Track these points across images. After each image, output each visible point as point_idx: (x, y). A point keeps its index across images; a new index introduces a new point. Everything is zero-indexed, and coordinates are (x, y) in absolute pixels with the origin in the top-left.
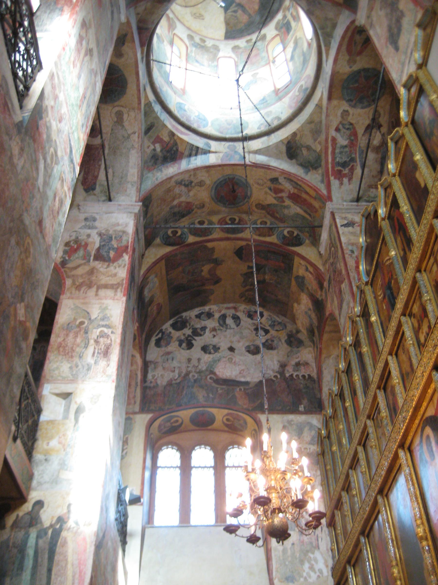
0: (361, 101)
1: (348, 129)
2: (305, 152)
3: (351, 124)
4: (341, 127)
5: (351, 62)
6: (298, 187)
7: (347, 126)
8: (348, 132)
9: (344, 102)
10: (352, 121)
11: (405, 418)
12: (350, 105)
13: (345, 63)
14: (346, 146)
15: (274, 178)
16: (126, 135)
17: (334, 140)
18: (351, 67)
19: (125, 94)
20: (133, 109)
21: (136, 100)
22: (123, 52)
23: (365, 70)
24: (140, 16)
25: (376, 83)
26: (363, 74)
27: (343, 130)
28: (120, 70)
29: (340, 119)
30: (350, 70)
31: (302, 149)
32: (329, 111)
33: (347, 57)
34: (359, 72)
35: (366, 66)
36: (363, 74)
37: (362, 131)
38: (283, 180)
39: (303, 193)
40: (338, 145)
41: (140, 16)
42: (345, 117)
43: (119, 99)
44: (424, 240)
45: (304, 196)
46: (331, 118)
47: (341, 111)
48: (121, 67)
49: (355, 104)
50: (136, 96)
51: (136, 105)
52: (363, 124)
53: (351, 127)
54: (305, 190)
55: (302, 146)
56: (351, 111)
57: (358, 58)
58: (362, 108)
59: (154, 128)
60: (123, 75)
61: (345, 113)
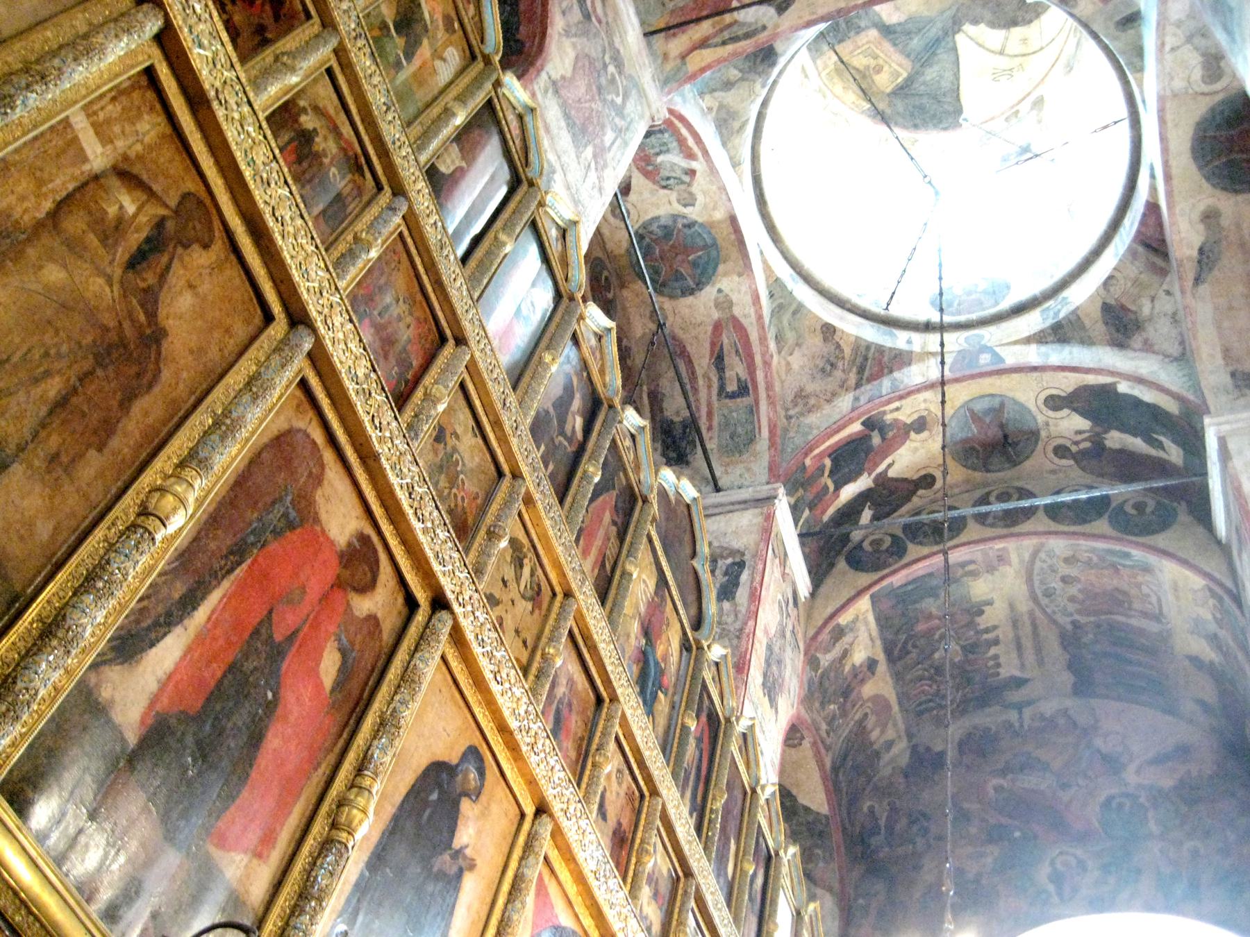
0: (668, 231)
1: (668, 178)
2: (734, 73)
3: (665, 187)
4: (686, 179)
5: (724, 303)
6: (726, 35)
7: (672, 182)
8: (665, 173)
9: (700, 220)
10: (666, 191)
11: (482, 643)
12: (684, 217)
13: (734, 297)
14: (658, 154)
15: (786, 8)
16: (1197, 40)
17: (690, 156)
18: (720, 291)
19: (1198, 124)
20: (1175, 95)
21: (1169, 117)
22: (1201, 227)
23: (692, 292)
24: (1165, 287)
25: (655, 272)
26: (691, 284)
27: (678, 173)
28: (1208, 179)
29: (695, 189)
30: (718, 286)
31: (740, 75)
32: (724, 197)
33: (737, 311)
34: (699, 286)
35: (690, 300)
36: (691, 284)
37: (634, 182)
38: (765, 21)
39: (711, 31)
40: (677, 151)
41: (1165, 287)
42: (686, 195)
43: (1213, 110)
44: (612, 677)
45: (706, 27)
46: (714, 188)
47: (700, 199)
48: (1205, 185)
49: (675, 221)
50: (1170, 124)
51: (1168, 105)
52: (641, 193)
53: (664, 183)
54: (709, 46)
55: (742, 79)
56: (678, 208)
57: (716, 315)
58: (657, 218)
59: (1118, 18)
60: (1200, 168)
61: (689, 201)
